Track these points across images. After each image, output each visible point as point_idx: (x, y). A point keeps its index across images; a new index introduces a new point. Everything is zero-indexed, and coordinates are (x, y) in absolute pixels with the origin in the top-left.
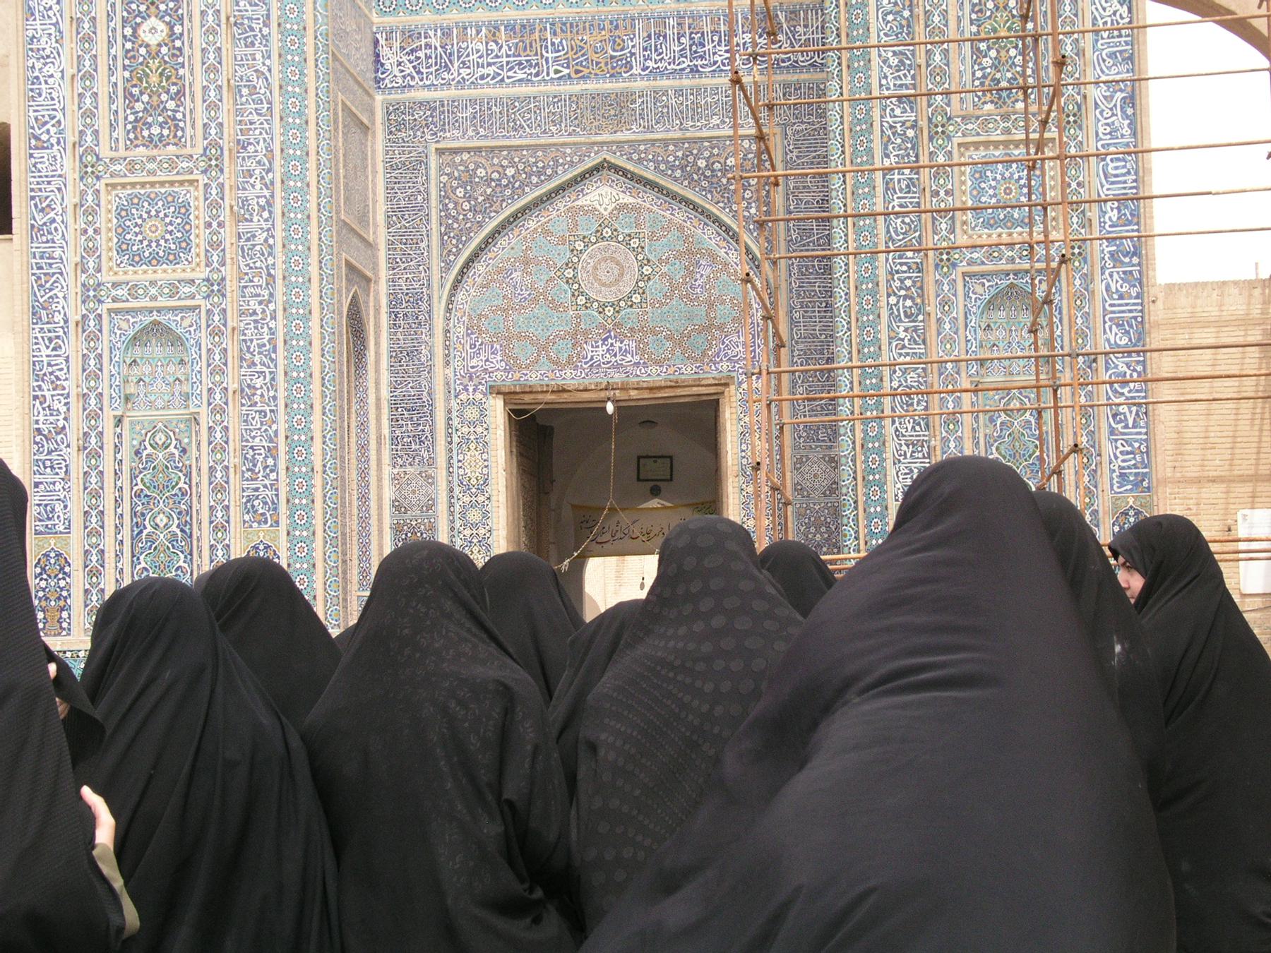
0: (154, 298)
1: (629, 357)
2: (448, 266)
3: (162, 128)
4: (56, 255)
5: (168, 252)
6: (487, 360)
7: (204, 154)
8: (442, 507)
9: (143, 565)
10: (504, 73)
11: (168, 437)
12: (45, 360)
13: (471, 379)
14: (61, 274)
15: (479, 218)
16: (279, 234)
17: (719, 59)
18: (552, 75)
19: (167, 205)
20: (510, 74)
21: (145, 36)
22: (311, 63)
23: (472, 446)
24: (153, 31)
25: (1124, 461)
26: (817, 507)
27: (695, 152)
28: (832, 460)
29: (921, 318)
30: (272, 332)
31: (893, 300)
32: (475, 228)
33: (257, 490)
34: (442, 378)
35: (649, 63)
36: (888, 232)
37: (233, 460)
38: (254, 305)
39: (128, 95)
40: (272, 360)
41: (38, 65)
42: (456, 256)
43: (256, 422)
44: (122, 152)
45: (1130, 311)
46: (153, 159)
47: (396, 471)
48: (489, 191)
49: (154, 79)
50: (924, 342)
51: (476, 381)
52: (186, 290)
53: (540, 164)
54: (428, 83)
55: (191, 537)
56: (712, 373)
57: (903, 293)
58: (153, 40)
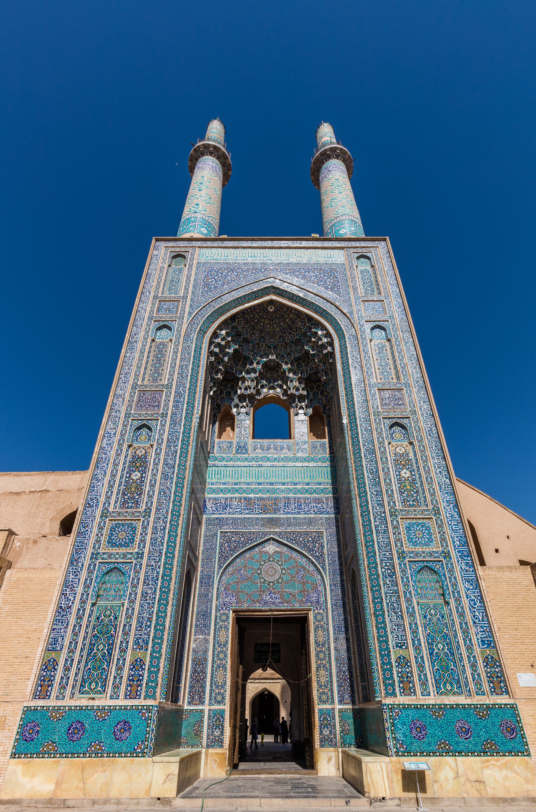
0: (117, 559)
3: (132, 503)
4: (85, 542)
5: (126, 543)
7: (145, 511)
9: (89, 666)
11: (111, 612)
12: (71, 579)
14: (85, 549)
16: (166, 538)
19: (129, 527)
21: (133, 477)
22: (185, 488)
24: (136, 476)
25: (481, 635)
29: (394, 577)
30: (158, 573)
31: (383, 570)
33: (141, 635)
36: (379, 546)
37: (134, 623)
38: (153, 563)
39: (124, 494)
40: (156, 583)
41: (95, 482)
43: (146, 607)
44: (117, 510)
45: (471, 577)
46: (127, 512)
49: (133, 489)
50: (397, 585)
51: (226, 606)
52: (129, 556)
55: (111, 655)
57: (387, 567)
58: (135, 478)
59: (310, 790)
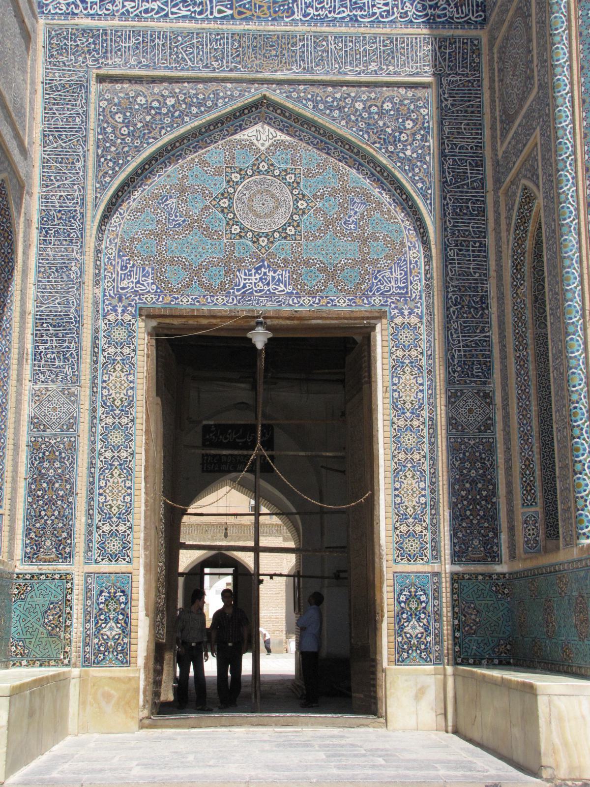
1: (282, 287)
2: (104, 187)
6: (138, 282)
8: (84, 427)
10: (168, 9)
13: (120, 300)
15: (137, 143)
17: (378, 11)
18: (216, 14)
20: (174, 10)
23: (118, 367)
26: (472, 442)
27: (353, 95)
28: (486, 396)
32: (132, 153)
34: (91, 296)
35: (311, 11)
42: (112, 177)
47: (37, 387)
48: (148, 118)
53: (201, 96)
54: (92, 12)
56: (363, 307)
59: (381, 761)
